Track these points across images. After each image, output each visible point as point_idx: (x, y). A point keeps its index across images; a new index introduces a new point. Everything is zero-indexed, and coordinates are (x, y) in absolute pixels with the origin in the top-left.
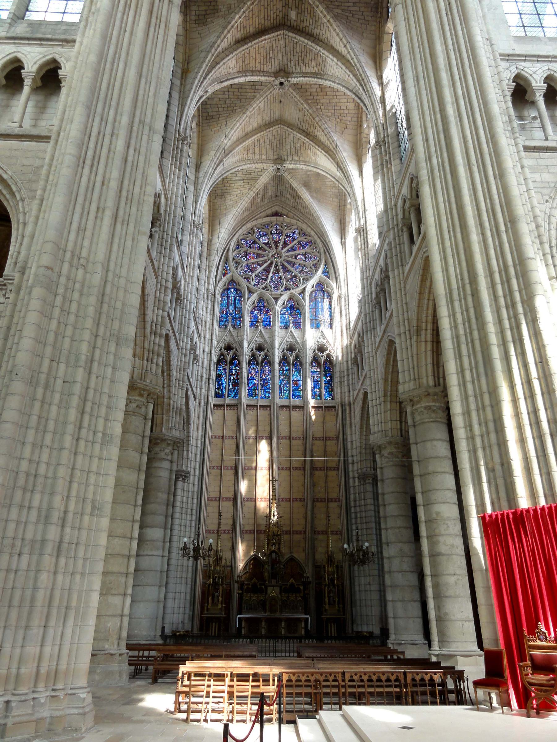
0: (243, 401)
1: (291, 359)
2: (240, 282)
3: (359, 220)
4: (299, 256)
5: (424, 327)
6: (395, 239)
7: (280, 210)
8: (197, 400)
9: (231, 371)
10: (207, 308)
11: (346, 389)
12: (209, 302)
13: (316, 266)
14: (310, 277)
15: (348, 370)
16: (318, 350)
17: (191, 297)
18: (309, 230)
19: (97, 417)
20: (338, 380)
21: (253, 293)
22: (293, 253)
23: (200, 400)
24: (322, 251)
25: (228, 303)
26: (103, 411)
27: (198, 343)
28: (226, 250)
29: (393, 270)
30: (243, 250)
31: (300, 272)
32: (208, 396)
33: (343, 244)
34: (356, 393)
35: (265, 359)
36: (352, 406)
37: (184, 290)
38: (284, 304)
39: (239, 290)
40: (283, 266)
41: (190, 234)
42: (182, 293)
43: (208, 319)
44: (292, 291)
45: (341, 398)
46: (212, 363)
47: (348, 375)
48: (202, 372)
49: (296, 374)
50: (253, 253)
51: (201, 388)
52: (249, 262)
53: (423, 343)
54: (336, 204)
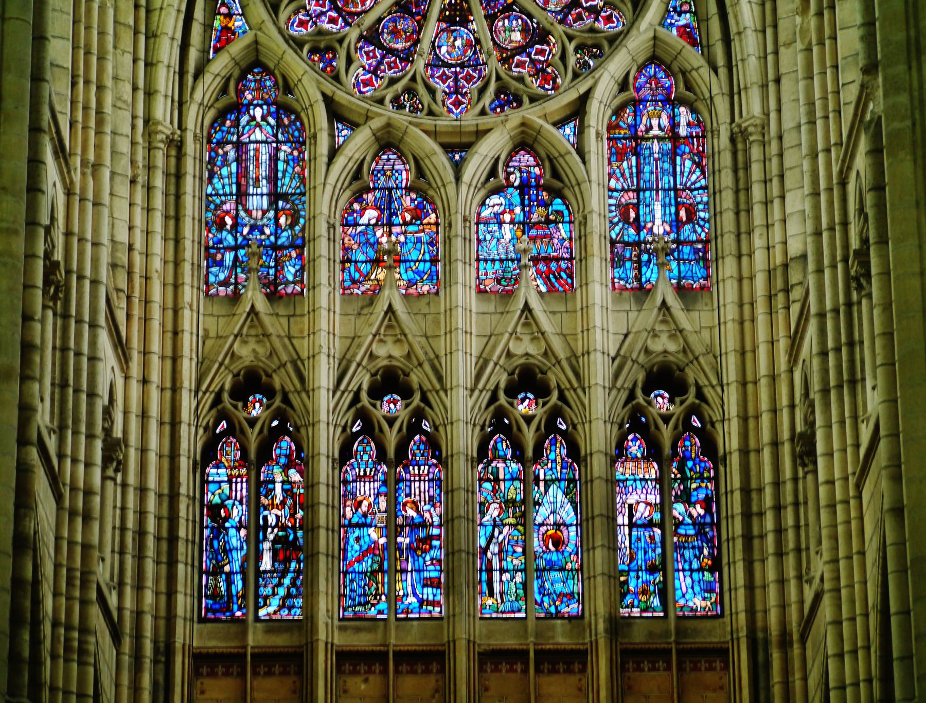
0: (322, 636)
1: (529, 436)
2: (293, 77)
8: (127, 643)
9: (261, 488)
10: (149, 210)
11: (771, 575)
14: (614, 40)
15: (777, 484)
20: (738, 527)
21: (353, 126)
23: (138, 636)
25: (242, 173)
32: (170, 618)
34: (809, 595)
35: (414, 428)
36: (796, 650)
37: (68, 234)
38: (493, 173)
39: (288, 110)
42: (58, 256)
43: (157, 264)
44: (532, 113)
45: (751, 611)
46: (184, 464)
47: (778, 508)
48: (142, 514)
49: (556, 494)
51: (139, 587)
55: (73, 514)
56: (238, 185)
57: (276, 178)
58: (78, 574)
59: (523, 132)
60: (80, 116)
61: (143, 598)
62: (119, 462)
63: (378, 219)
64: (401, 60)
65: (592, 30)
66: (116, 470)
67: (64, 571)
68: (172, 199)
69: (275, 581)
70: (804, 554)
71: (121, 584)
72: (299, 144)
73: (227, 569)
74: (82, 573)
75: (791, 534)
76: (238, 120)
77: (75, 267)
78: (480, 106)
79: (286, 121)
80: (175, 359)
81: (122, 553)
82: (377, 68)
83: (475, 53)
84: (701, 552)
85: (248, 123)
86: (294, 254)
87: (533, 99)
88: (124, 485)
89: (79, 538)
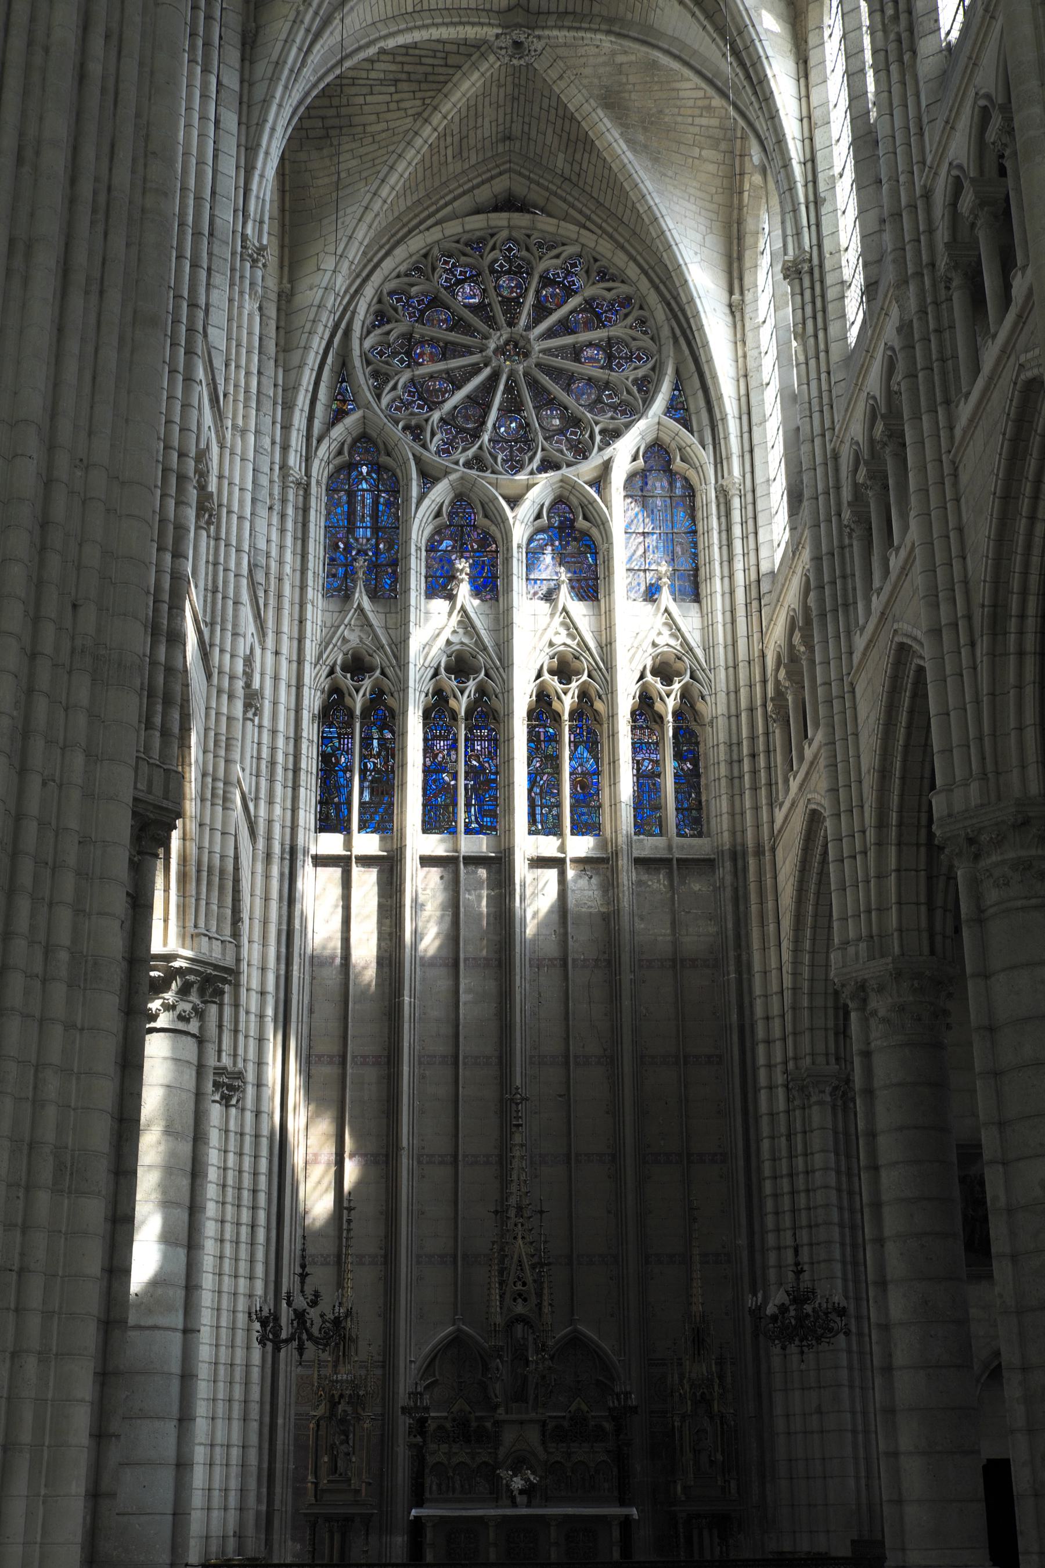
3: (798, 234)
4: (589, 352)
5: (1014, 608)
6: (923, 311)
7: (520, 188)
12: (290, 511)
13: (647, 388)
15: (753, 738)
16: (655, 672)
17: (241, 502)
18: (620, 259)
19: (51, 905)
20: (723, 770)
22: (569, 340)
23: (269, 839)
24: (665, 332)
25: (351, 514)
26: (68, 883)
27: (258, 651)
28: (342, 330)
29: (917, 417)
30: (398, 329)
31: (591, 409)
32: (294, 827)
33: (737, 311)
37: (220, 477)
38: (539, 516)
39: (387, 469)
40: (534, 385)
41: (232, 285)
46: (306, 715)
47: (753, 756)
48: (273, 749)
50: (433, 341)
51: (271, 802)
52: (421, 371)
53: (1012, 660)
54: (712, 168)
55: (220, 691)
56: (349, 523)
57: (377, 517)
58: (224, 738)
59: (561, 487)
60: (231, 390)
61: (273, 811)
62: (257, 709)
63: (453, 547)
64: (471, 436)
66: (255, 714)
67: (212, 734)
68: (300, 525)
69: (372, 810)
70: (774, 787)
71: (257, 798)
73: (336, 800)
74: (227, 739)
75: (763, 774)
76: (349, 474)
77: (225, 502)
78: (529, 469)
79: (385, 476)
80: (301, 640)
81: (258, 776)
82: (452, 441)
83: (526, 432)
84: (690, 796)
85: (357, 477)
86: (390, 570)
87: (569, 465)
88: (260, 727)
89: (225, 710)
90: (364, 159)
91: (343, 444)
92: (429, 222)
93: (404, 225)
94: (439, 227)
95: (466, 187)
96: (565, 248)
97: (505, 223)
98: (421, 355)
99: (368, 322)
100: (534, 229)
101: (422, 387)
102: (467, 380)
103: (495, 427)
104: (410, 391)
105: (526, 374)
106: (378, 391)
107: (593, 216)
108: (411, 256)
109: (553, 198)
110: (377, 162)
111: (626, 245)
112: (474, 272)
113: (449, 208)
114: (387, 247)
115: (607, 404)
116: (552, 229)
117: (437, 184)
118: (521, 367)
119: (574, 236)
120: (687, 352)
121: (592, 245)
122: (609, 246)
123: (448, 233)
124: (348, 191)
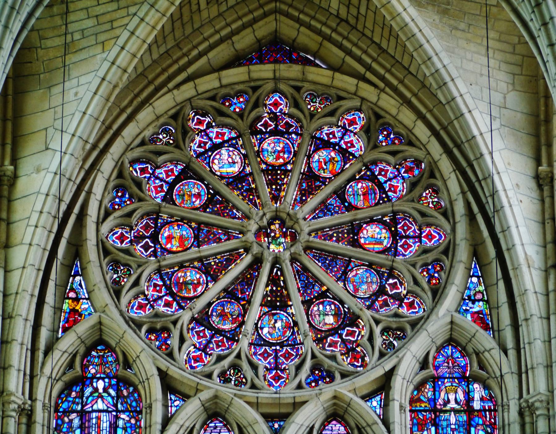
2: (132, 355)
14: (414, 324)
21: (185, 397)
22: (347, 217)
39: (128, 383)
52: (170, 259)
59: (335, 404)
64: (228, 339)
65: (396, 315)
72: (136, 413)
76: (82, 391)
79: (125, 393)
82: (206, 346)
83: (293, 334)
85: (92, 394)
87: (344, 375)
90: (102, 19)
91: (75, 356)
92: (180, 78)
93: (150, 83)
94: (191, 84)
95: (224, 33)
96: (342, 103)
97: (270, 75)
98: (170, 238)
99: (106, 202)
100: (304, 80)
101: (170, 279)
102: (224, 266)
103: (257, 328)
104: (155, 285)
105: (294, 259)
106: (116, 287)
107: (375, 65)
108: (158, 118)
109: (327, 44)
110: (115, 24)
111: (414, 101)
112: (233, 135)
113: (204, 60)
114: (129, 111)
115: (390, 296)
116: (326, 81)
117: (189, 30)
118: (287, 255)
119: (353, 89)
120: (486, 233)
121: (374, 99)
122: (393, 102)
123: (201, 89)
124: (83, 55)
